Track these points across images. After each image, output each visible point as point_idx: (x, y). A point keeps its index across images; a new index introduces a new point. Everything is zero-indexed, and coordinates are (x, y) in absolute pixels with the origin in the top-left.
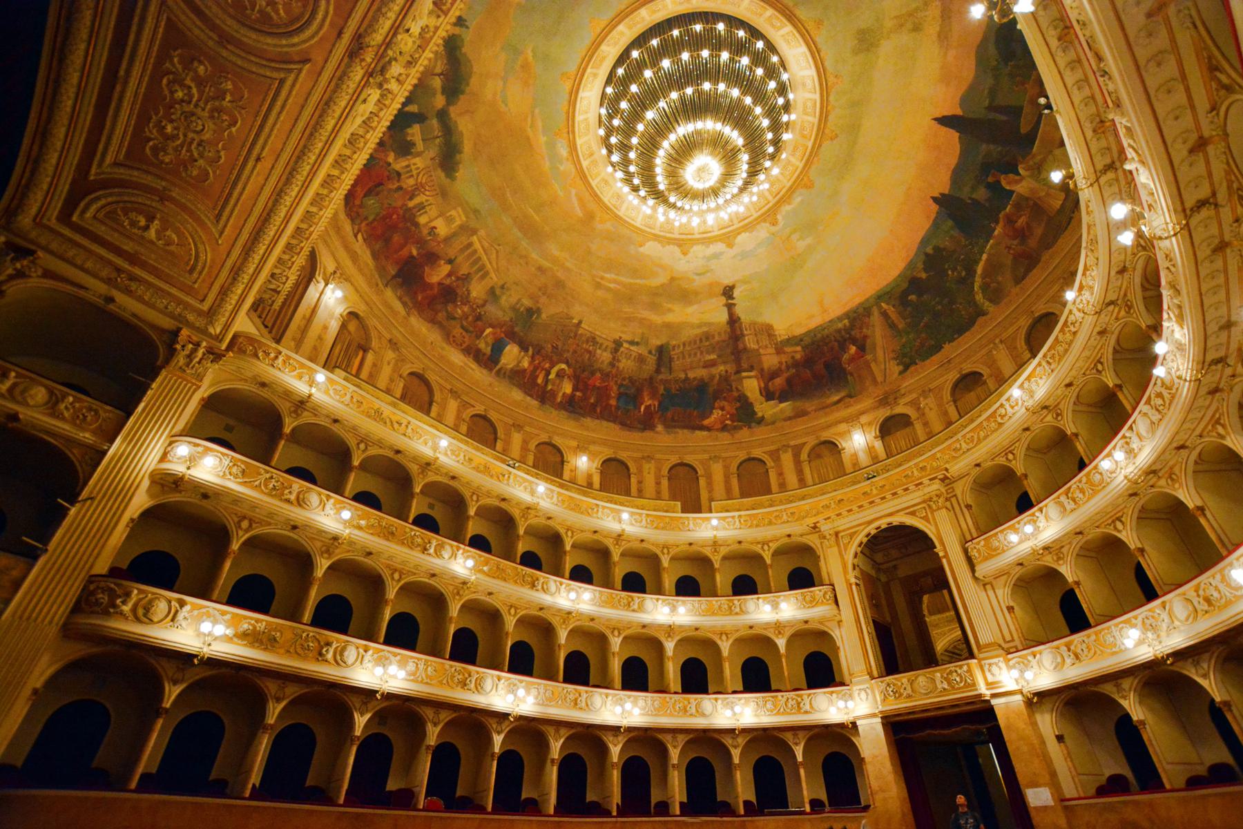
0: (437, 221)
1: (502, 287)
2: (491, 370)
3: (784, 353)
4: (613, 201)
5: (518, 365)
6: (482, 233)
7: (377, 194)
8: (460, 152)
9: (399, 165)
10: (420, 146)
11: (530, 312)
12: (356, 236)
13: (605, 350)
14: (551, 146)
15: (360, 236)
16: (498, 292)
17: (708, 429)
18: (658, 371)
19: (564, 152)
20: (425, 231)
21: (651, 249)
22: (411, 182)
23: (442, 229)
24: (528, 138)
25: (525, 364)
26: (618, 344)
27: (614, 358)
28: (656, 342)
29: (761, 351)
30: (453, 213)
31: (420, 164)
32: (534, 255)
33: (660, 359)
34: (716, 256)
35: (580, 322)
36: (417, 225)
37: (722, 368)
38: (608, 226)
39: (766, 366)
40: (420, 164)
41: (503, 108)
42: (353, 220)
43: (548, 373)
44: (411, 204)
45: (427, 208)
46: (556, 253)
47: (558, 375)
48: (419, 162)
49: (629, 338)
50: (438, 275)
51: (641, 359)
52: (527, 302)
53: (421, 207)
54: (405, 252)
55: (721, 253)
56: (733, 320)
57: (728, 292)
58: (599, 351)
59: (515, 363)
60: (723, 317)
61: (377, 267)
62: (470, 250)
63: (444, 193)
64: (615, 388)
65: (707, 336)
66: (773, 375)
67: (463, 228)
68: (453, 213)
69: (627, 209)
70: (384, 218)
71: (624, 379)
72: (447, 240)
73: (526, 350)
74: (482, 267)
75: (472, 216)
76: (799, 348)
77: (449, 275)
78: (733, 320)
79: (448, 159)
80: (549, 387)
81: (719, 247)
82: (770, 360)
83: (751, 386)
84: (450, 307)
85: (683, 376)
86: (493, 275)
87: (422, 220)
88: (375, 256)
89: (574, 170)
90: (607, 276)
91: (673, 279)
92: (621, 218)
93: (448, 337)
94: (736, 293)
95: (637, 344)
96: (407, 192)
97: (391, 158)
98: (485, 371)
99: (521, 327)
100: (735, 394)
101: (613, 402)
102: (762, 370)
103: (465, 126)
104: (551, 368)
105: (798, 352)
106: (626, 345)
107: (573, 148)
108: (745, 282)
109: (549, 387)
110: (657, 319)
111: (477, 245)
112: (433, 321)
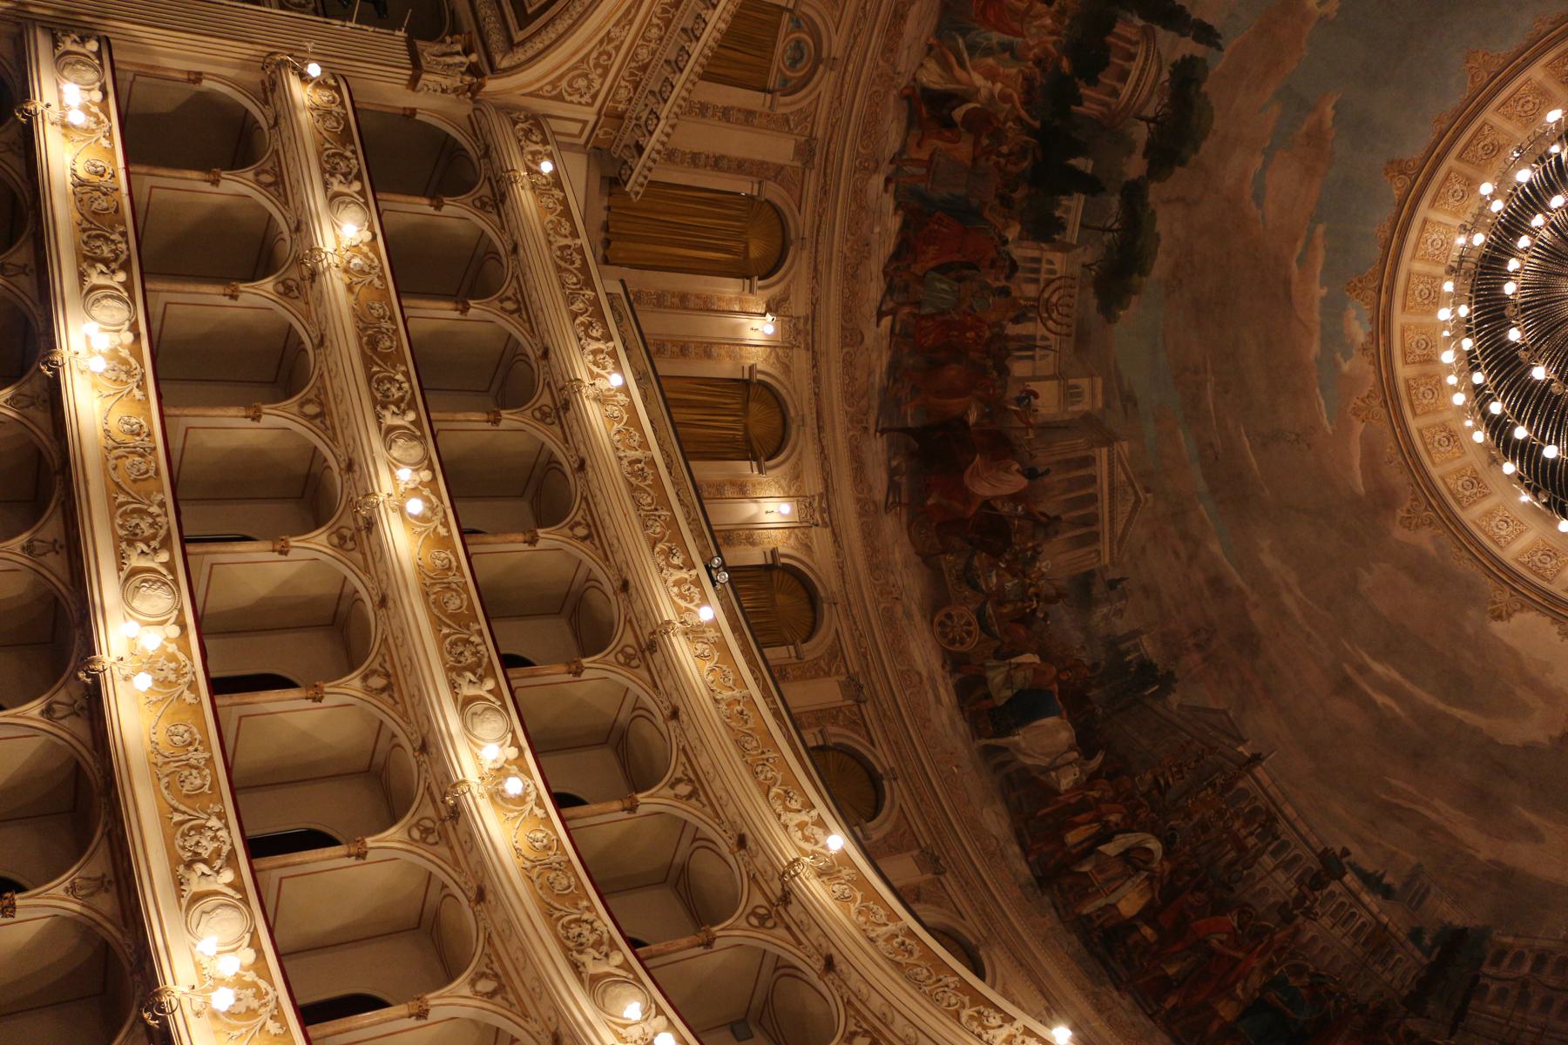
0: (1046, 388)
1: (1112, 585)
2: (977, 733)
4: (1457, 484)
5: (1045, 770)
6: (1124, 447)
7: (960, 280)
8: (1144, 272)
9: (1022, 252)
10: (1072, 234)
11: (1146, 669)
12: (880, 315)
13: (1287, 866)
14: (1334, 309)
15: (887, 321)
16: (1098, 590)
19: (1359, 331)
20: (1013, 392)
21: (1526, 633)
22: (1031, 290)
23: (1048, 401)
24: (1287, 282)
25: (1066, 781)
26: (1331, 865)
27: (1300, 900)
28: (1448, 912)
31: (1061, 264)
35: (1256, 759)
36: (1004, 371)
38: (1424, 538)
40: (1061, 264)
42: (890, 290)
43: (1106, 837)
44: (1012, 330)
46: (1269, 561)
47: (1126, 856)
48: (1057, 262)
49: (1369, 866)
50: (993, 484)
51: (1378, 941)
52: (1149, 648)
58: (1267, 860)
59: (1044, 762)
61: (885, 390)
62: (1082, 472)
64: (1256, 980)
67: (1086, 418)
68: (1084, 383)
69: (1489, 514)
71: (1298, 971)
72: (1050, 428)
73: (1088, 754)
74: (1090, 520)
77: (1015, 498)
79: (1117, 277)
80: (1086, 868)
84: (981, 559)
86: (1105, 547)
87: (1019, 369)
88: (894, 368)
89: (1372, 378)
90: (1378, 668)
92: (1461, 526)
93: (937, 604)
95: (1387, 892)
97: (1012, 233)
98: (962, 726)
99: (1111, 695)
101: (1227, 1011)
103: (1168, 224)
104: (1127, 830)
107: (1382, 325)
109: (1086, 868)
110: (1485, 849)
111: (1102, 469)
112: (927, 558)
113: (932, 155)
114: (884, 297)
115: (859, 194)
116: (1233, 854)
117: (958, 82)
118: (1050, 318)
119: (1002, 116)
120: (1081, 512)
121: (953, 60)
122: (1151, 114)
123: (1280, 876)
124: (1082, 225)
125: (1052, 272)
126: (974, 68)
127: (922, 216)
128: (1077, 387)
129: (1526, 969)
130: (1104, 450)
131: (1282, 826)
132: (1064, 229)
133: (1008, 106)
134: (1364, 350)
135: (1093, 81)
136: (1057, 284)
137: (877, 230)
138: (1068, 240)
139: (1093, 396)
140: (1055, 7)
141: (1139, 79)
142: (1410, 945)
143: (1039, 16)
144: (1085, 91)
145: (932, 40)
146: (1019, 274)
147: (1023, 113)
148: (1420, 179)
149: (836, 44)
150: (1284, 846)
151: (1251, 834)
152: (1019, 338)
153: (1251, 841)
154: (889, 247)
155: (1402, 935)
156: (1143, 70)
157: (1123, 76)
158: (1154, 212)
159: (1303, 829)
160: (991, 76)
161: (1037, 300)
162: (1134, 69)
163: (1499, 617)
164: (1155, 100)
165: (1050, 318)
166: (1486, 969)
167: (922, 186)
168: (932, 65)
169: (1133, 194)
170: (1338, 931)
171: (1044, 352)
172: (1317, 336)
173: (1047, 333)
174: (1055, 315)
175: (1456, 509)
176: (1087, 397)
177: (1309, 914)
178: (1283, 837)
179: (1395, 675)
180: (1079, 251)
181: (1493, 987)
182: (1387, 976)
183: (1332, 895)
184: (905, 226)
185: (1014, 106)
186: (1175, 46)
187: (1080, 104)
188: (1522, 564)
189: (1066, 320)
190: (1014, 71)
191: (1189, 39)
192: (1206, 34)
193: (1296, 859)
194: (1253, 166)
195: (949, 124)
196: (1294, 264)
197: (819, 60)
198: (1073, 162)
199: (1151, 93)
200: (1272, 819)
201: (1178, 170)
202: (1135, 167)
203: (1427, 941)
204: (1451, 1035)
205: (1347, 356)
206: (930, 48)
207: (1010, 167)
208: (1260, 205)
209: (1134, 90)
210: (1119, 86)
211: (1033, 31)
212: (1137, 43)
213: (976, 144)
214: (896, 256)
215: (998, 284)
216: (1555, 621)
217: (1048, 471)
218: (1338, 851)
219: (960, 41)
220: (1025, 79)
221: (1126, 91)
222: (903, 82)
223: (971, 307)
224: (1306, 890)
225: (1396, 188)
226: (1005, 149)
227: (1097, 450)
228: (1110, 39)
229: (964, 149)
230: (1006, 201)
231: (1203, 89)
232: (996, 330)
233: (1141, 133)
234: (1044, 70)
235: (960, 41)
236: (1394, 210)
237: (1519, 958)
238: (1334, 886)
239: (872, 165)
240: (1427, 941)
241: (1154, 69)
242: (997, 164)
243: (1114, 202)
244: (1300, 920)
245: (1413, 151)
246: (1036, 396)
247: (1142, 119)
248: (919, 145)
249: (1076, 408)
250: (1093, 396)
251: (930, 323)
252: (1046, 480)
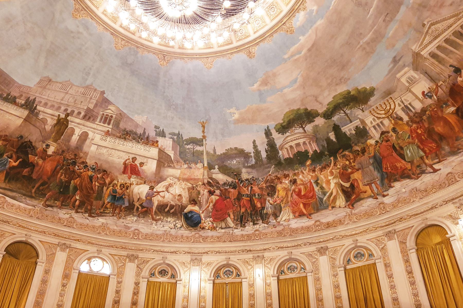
0: (416, 92)
6: (415, 48)
7: (402, 148)
8: (349, 92)
9: (375, 135)
10: (357, 123)
12: (435, 171)
14: (303, 30)
19: (301, 17)
20: (429, 101)
24: (309, 50)
30: (403, 80)
36: (424, 111)
41: (300, 79)
42: (423, 172)
44: (406, 118)
45: (406, 103)
48: (369, 121)
53: (406, 109)
54: (452, 120)
63: (388, 93)
67: (416, 69)
68: (403, 80)
70: (421, 141)
72: (432, 79)
75: (401, 63)
87: (418, 106)
96: (396, 123)
97: (371, 142)
103: (326, 99)
107: (292, 12)
111: (432, 47)
113: (366, 185)
114: (427, 173)
115: (395, 206)
117: (337, 191)
118: (390, 108)
119: (338, 171)
120: (458, 40)
121: (332, 198)
122: (301, 129)
124: (351, 122)
125: (374, 120)
126: (330, 189)
127: (389, 177)
128: (408, 82)
130: (422, 53)
132: (357, 126)
133: (333, 171)
135: (307, 152)
136: (376, 115)
137: (404, 190)
138: (360, 123)
139: (405, 73)
140: (295, 177)
141: (295, 140)
143: (302, 181)
144: (311, 152)
145: (330, 208)
146: (384, 129)
147: (332, 164)
148: (247, 46)
149: (348, 243)
152: (408, 114)
154: (406, 182)
156: (291, 141)
157: (298, 145)
158: (328, 105)
160: (328, 182)
161: (388, 117)
162: (293, 144)
164: (296, 131)
165: (390, 108)
167: (378, 182)
168: (338, 203)
169: (328, 115)
171: (404, 102)
172: (315, 26)
173: (397, 105)
174: (388, 108)
176: (407, 75)
180: (359, 116)
184: (396, 180)
185: (332, 169)
186: (278, 139)
187: (316, 150)
189: (387, 103)
190: (322, 176)
191: (273, 136)
192: (268, 133)
194: (289, 90)
195: (352, 186)
196: (303, 53)
197: (356, 247)
198: (334, 140)
199: (296, 134)
201: (309, 109)
202: (320, 121)
205: (312, 11)
206: (333, 207)
207: (352, 157)
208: (297, 79)
209: (299, 139)
210: (302, 144)
211: (306, 179)
212: (286, 148)
213: (352, 173)
214: (409, 177)
215: (393, 134)
217: (451, 66)
219: (325, 199)
220: (322, 172)
221: (301, 141)
222: (348, 210)
223: (409, 138)
225: (255, 50)
226: (347, 163)
227: (425, 56)
228: (291, 156)
229: (357, 176)
230: (364, 151)
231: (282, 122)
232: (410, 124)
233: (309, 128)
234: (315, 168)
235: (325, 199)
236: (261, 44)
239: (382, 206)
241: (289, 138)
242: (354, 162)
243: (335, 118)
245: (243, 56)
246: (423, 93)
247: (305, 131)
248: (365, 192)
249: (416, 75)
250: (405, 73)
251: (426, 149)
252: (455, 64)
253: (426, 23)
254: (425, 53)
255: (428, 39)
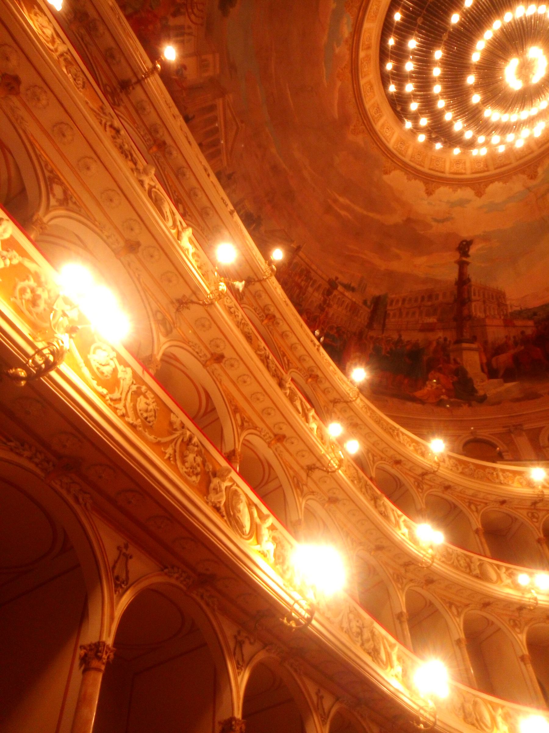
3: (514, 326)
6: (230, 97)
13: (317, 289)
17: (422, 402)
18: (370, 326)
19: (346, 31)
21: (396, 179)
26: (333, 285)
27: (325, 301)
28: (374, 291)
29: (488, 322)
32: (273, 150)
33: (374, 312)
34: (462, 203)
37: (440, 334)
38: (360, 140)
39: (491, 337)
49: (346, 282)
51: (354, 308)
55: (468, 201)
56: (463, 281)
57: (464, 247)
58: (310, 289)
60: (452, 275)
65: (431, 295)
66: (499, 350)
71: (331, 328)
76: (531, 323)
78: (463, 281)
81: (467, 193)
82: (496, 332)
83: (472, 360)
85: (395, 337)
89: (347, 57)
90: (341, 200)
91: (409, 220)
94: (472, 251)
95: (353, 290)
100: (452, 366)
102: (486, 342)
105: (529, 328)
106: (340, 288)
108: (486, 238)
110: (381, 264)
116: (298, 291)
118: (193, 13)
123: (316, 294)
129: (400, 304)
131: (313, 274)
134: (347, 41)
142: (364, 306)
150: (315, 281)
151: (302, 280)
153: (303, 284)
155: (361, 304)
159: (320, 272)
163: (386, 173)
165: (193, 13)
166: (389, 308)
170: (340, 309)
173: (190, 24)
174: (195, 11)
175: (373, 123)
177: (329, 306)
178: (314, 279)
179: (348, 202)
181: (391, 313)
182: (359, 320)
183: (335, 296)
188: (395, 149)
193: (320, 286)
200: (308, 272)
203: (369, 303)
204: (383, 333)
216: (406, 174)
217: (194, 117)
218: (334, 278)
223: (151, 6)
224: (326, 297)
237: (398, 301)
238: (335, 292)
240: (369, 303)
244: (327, 309)
253: (243, 125)
254: (220, 102)
255: (229, 115)
